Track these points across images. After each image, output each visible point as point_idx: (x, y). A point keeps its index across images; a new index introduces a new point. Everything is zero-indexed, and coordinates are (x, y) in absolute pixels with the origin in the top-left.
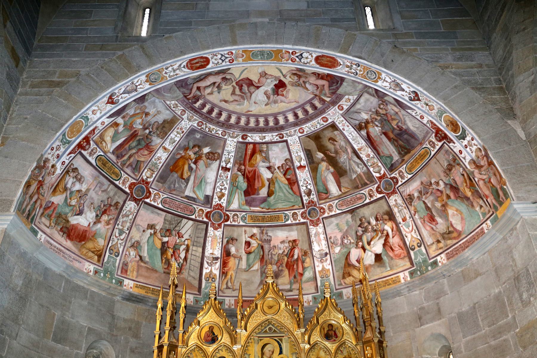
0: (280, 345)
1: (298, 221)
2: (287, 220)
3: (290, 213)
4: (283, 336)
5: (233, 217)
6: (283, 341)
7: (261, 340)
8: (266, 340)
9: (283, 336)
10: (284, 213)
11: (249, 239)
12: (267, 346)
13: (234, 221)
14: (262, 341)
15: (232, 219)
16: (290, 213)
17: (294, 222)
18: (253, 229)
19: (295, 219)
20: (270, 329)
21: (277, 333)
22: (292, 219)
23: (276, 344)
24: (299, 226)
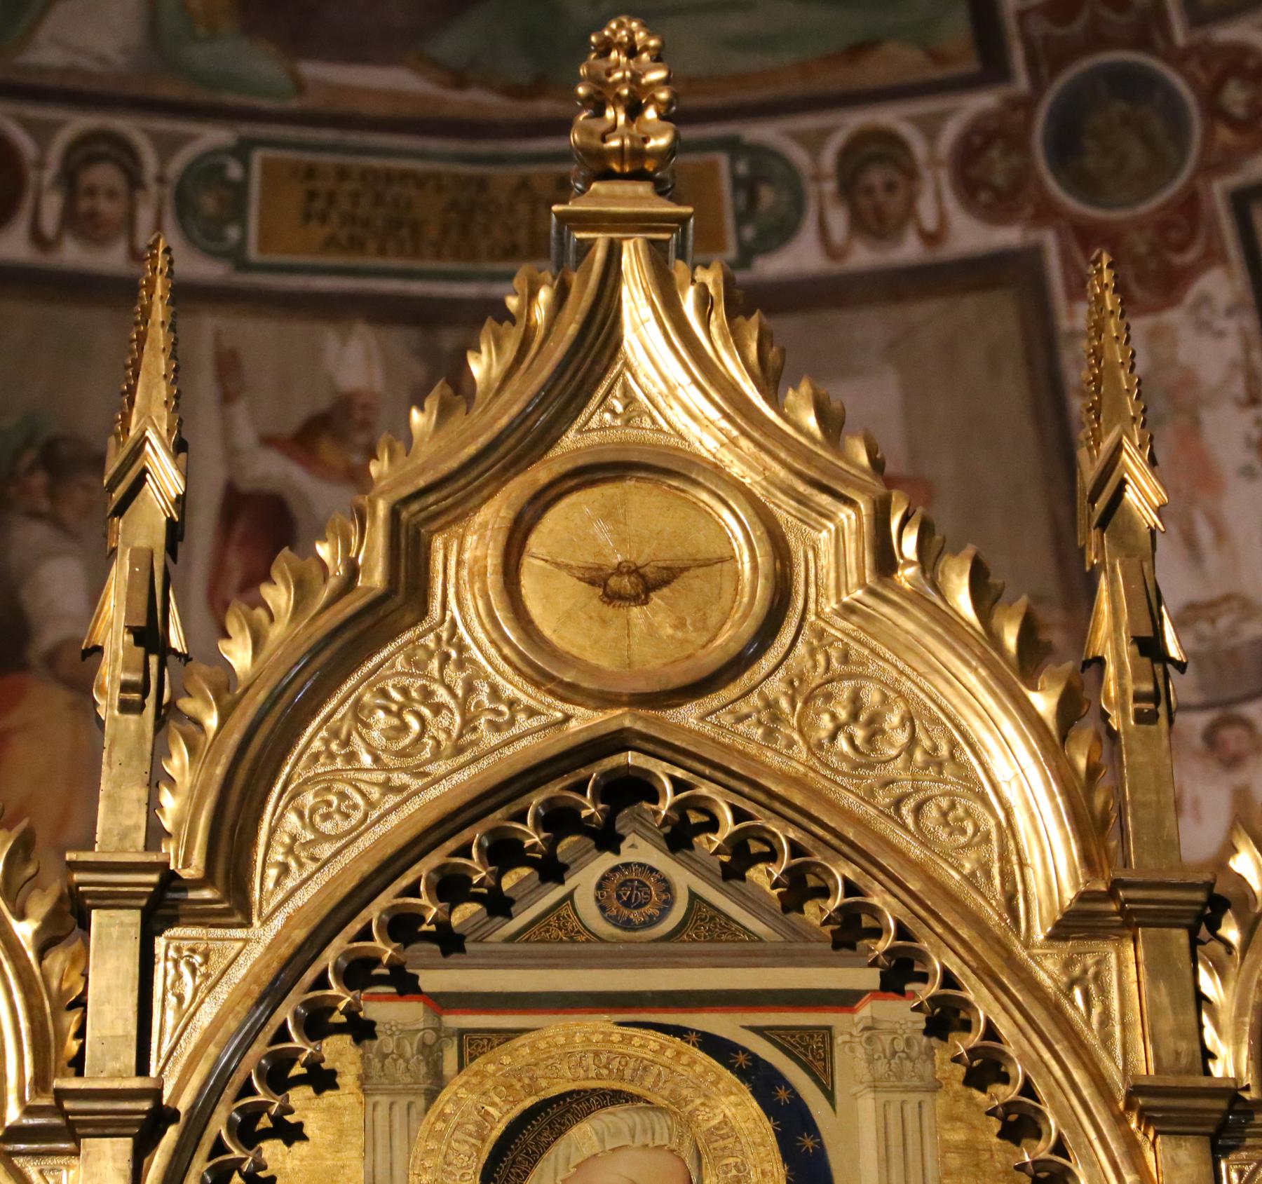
0: (794, 1127)
1: (909, 250)
2: (779, 233)
3: (813, 142)
4: (846, 1000)
5: (69, 178)
6: (850, 1061)
7: (473, 1045)
8: (567, 1048)
9: (846, 1000)
10: (733, 146)
11: (270, 469)
12: (584, 1135)
13: (80, 222)
14: (491, 1065)
15: (52, 206)
16: (813, 142)
17: (863, 257)
18: (330, 338)
19: (874, 224)
20: (629, 893)
21: (753, 952)
22: (838, 221)
23: (736, 1109)
24: (921, 312)
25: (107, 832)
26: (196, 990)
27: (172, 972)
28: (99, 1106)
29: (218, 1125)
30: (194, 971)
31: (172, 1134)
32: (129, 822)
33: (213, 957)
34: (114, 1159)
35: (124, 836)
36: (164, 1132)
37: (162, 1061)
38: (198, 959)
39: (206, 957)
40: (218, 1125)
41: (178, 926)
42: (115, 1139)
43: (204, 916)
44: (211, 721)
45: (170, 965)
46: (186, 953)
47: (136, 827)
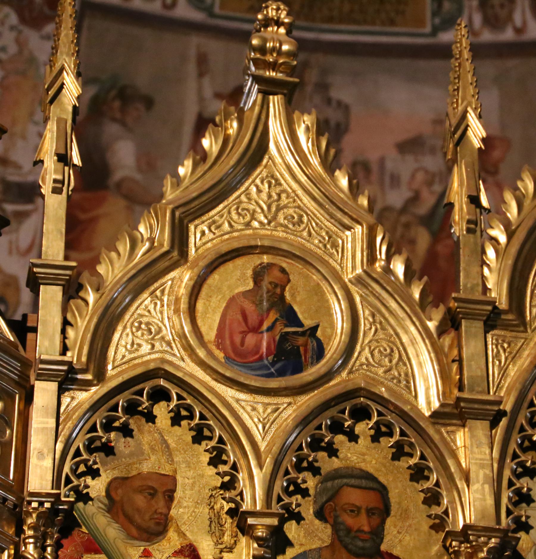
25: (465, 286)
26: (506, 359)
27: (495, 350)
28: (476, 406)
29: (522, 420)
30: (505, 350)
31: (504, 422)
32: (475, 282)
33: (513, 345)
34: (483, 430)
35: (472, 288)
36: (501, 420)
37: (495, 388)
38: (506, 345)
39: (509, 346)
40: (522, 420)
41: (496, 329)
42: (482, 421)
43: (507, 327)
44: (503, 239)
45: (494, 347)
46: (500, 341)
47: (478, 285)
